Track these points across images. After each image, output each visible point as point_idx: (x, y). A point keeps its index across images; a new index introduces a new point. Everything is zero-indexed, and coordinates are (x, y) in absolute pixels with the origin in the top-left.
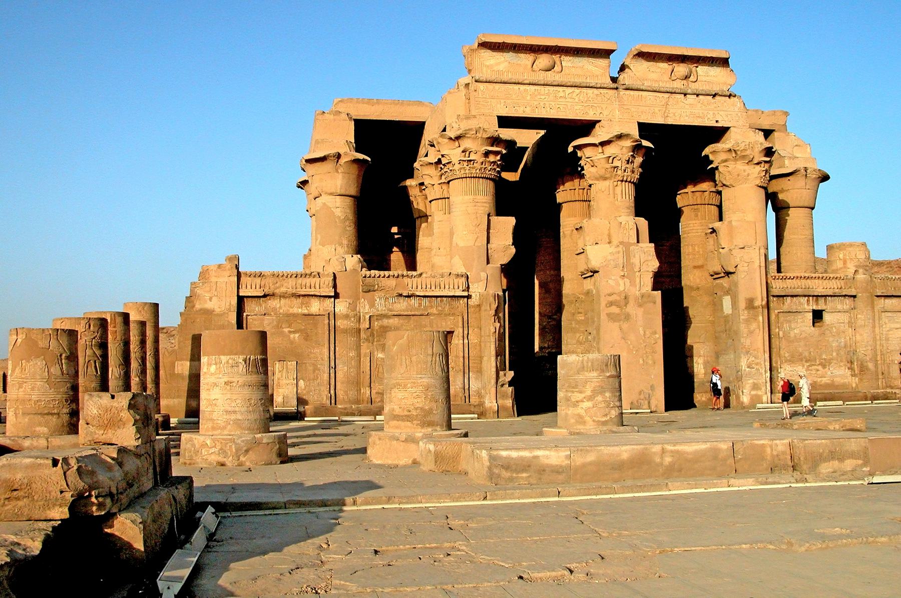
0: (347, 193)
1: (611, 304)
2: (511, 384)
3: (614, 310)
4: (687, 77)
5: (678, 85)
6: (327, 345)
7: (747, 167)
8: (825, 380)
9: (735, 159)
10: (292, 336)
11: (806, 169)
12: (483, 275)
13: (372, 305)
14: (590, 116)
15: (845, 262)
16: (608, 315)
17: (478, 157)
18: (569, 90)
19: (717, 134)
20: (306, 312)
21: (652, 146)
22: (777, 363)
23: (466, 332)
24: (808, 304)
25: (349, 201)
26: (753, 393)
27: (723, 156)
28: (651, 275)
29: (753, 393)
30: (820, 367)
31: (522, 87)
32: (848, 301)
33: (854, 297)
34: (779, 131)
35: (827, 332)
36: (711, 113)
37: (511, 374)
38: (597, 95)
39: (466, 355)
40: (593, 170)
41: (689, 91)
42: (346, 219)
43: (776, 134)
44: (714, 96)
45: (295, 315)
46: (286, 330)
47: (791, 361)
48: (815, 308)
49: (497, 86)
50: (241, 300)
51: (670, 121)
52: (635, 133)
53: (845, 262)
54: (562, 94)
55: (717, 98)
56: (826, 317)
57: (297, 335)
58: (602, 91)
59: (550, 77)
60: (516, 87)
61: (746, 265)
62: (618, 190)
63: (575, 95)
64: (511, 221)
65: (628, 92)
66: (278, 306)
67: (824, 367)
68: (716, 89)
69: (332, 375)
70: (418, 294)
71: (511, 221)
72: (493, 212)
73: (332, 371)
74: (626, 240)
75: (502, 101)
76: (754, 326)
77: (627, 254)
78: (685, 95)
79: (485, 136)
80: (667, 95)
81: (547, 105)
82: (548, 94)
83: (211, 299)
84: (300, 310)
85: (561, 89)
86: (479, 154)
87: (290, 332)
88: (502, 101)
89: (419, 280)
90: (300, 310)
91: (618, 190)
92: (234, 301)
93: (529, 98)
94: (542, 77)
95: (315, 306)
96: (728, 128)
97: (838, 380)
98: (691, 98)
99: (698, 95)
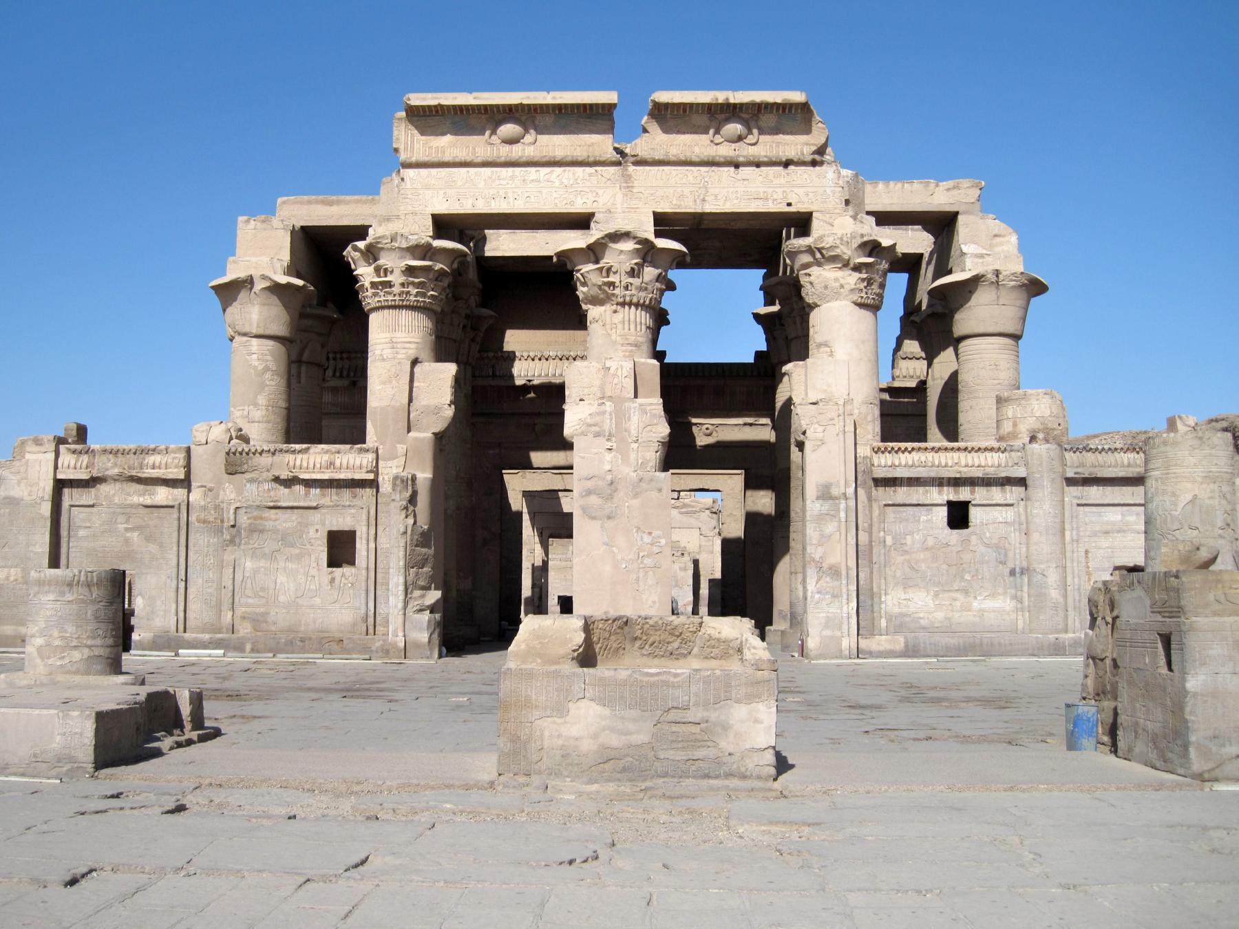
0: (268, 332)
1: (589, 492)
2: (433, 609)
3: (594, 500)
6: (175, 548)
7: (840, 274)
8: (969, 617)
9: (819, 264)
10: (128, 535)
11: (997, 273)
12: (401, 448)
13: (240, 491)
14: (578, 206)
15: (1015, 425)
16: (584, 510)
17: (396, 278)
18: (544, 171)
19: (802, 223)
20: (149, 502)
21: (684, 249)
22: (879, 587)
23: (372, 532)
24: (940, 493)
26: (828, 633)
27: (806, 258)
28: (656, 446)
29: (828, 633)
32: (1018, 491)
33: (1022, 482)
34: (966, 213)
35: (974, 538)
37: (434, 595)
38: (590, 175)
39: (372, 566)
40: (585, 289)
41: (741, 159)
43: (960, 217)
45: (132, 506)
46: (121, 527)
47: (907, 584)
48: (953, 497)
50: (60, 485)
51: (709, 208)
52: (647, 230)
53: (1015, 425)
55: (791, 167)
56: (975, 514)
57: (136, 534)
59: (516, 151)
61: (820, 429)
62: (619, 316)
64: (451, 369)
66: (112, 492)
67: (966, 592)
69: (182, 591)
70: (301, 477)
71: (451, 369)
72: (425, 354)
73: (182, 585)
76: (830, 527)
77: (621, 416)
81: (510, 195)
82: (512, 178)
83: (19, 483)
84: (141, 499)
85: (533, 170)
86: (397, 272)
87: (127, 530)
89: (305, 456)
90: (141, 499)
92: (49, 486)
94: (506, 152)
95: (162, 495)
96: (810, 214)
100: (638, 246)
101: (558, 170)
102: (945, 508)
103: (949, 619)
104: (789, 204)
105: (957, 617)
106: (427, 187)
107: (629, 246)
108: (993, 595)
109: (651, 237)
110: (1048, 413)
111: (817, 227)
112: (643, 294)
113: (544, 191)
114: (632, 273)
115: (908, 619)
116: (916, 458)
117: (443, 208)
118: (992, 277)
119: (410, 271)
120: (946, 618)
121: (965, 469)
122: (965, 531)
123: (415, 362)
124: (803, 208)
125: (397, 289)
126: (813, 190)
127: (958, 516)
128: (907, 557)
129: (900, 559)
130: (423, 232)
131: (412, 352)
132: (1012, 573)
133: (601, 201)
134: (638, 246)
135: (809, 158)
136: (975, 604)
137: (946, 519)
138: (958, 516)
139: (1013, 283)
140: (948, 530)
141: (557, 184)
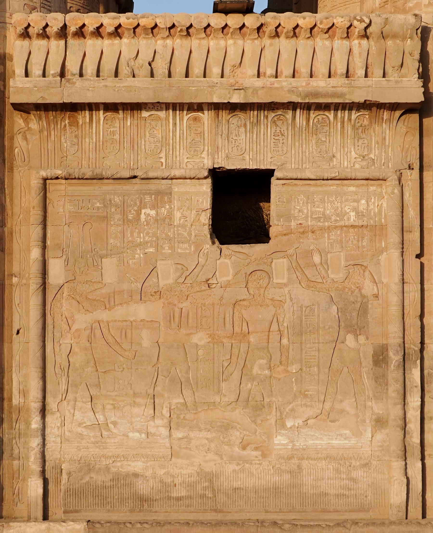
30: (238, 415)
35: (280, 264)
67: (258, 409)
97: (322, 479)
102: (206, 187)
103: (211, 478)
105: (232, 475)
108: (328, 418)
115: (99, 478)
116: (127, 54)
120: (201, 473)
121: (258, 83)
122: (258, 249)
127: (240, 205)
128: (104, 315)
129: (82, 320)
132: (380, 357)
136: (280, 440)
137: (206, 218)
138: (240, 205)
140: (210, 248)
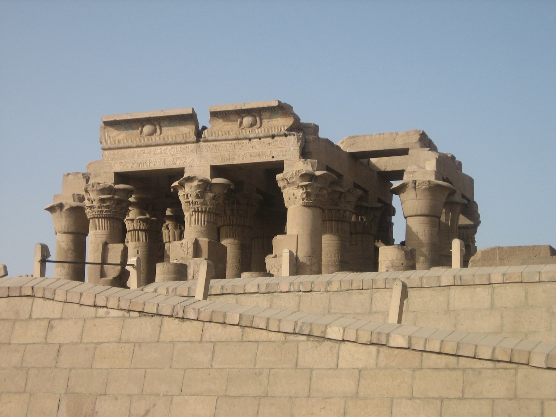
4: (252, 126)
5: (244, 133)
11: (415, 182)
14: (178, 165)
17: (95, 204)
25: (70, 237)
31: (132, 150)
34: (412, 148)
36: (269, 151)
38: (184, 149)
42: (69, 249)
44: (273, 137)
49: (116, 151)
51: (235, 162)
52: (207, 174)
54: (159, 151)
55: (276, 138)
58: (187, 145)
60: (129, 150)
61: (276, 270)
62: (193, 218)
63: (168, 150)
65: (206, 144)
68: (275, 132)
74: (185, 256)
75: (119, 161)
78: (250, 140)
79: (98, 188)
80: (235, 142)
81: (148, 161)
85: (158, 148)
86: (96, 201)
88: (119, 161)
91: (193, 218)
93: (136, 157)
98: (255, 142)
99: (250, 140)
100: (199, 183)
101: (169, 147)
104: (273, 157)
106: (113, 159)
107: (196, 183)
109: (209, 178)
110: (395, 258)
111: (286, 168)
112: (204, 207)
113: (163, 158)
114: (197, 196)
117: (119, 169)
118: (411, 185)
119: (102, 200)
123: (105, 245)
124: (279, 159)
125: (96, 209)
126: (286, 148)
130: (109, 181)
131: (103, 239)
133: (188, 161)
134: (199, 183)
135: (282, 133)
139: (424, 187)
141: (168, 155)
